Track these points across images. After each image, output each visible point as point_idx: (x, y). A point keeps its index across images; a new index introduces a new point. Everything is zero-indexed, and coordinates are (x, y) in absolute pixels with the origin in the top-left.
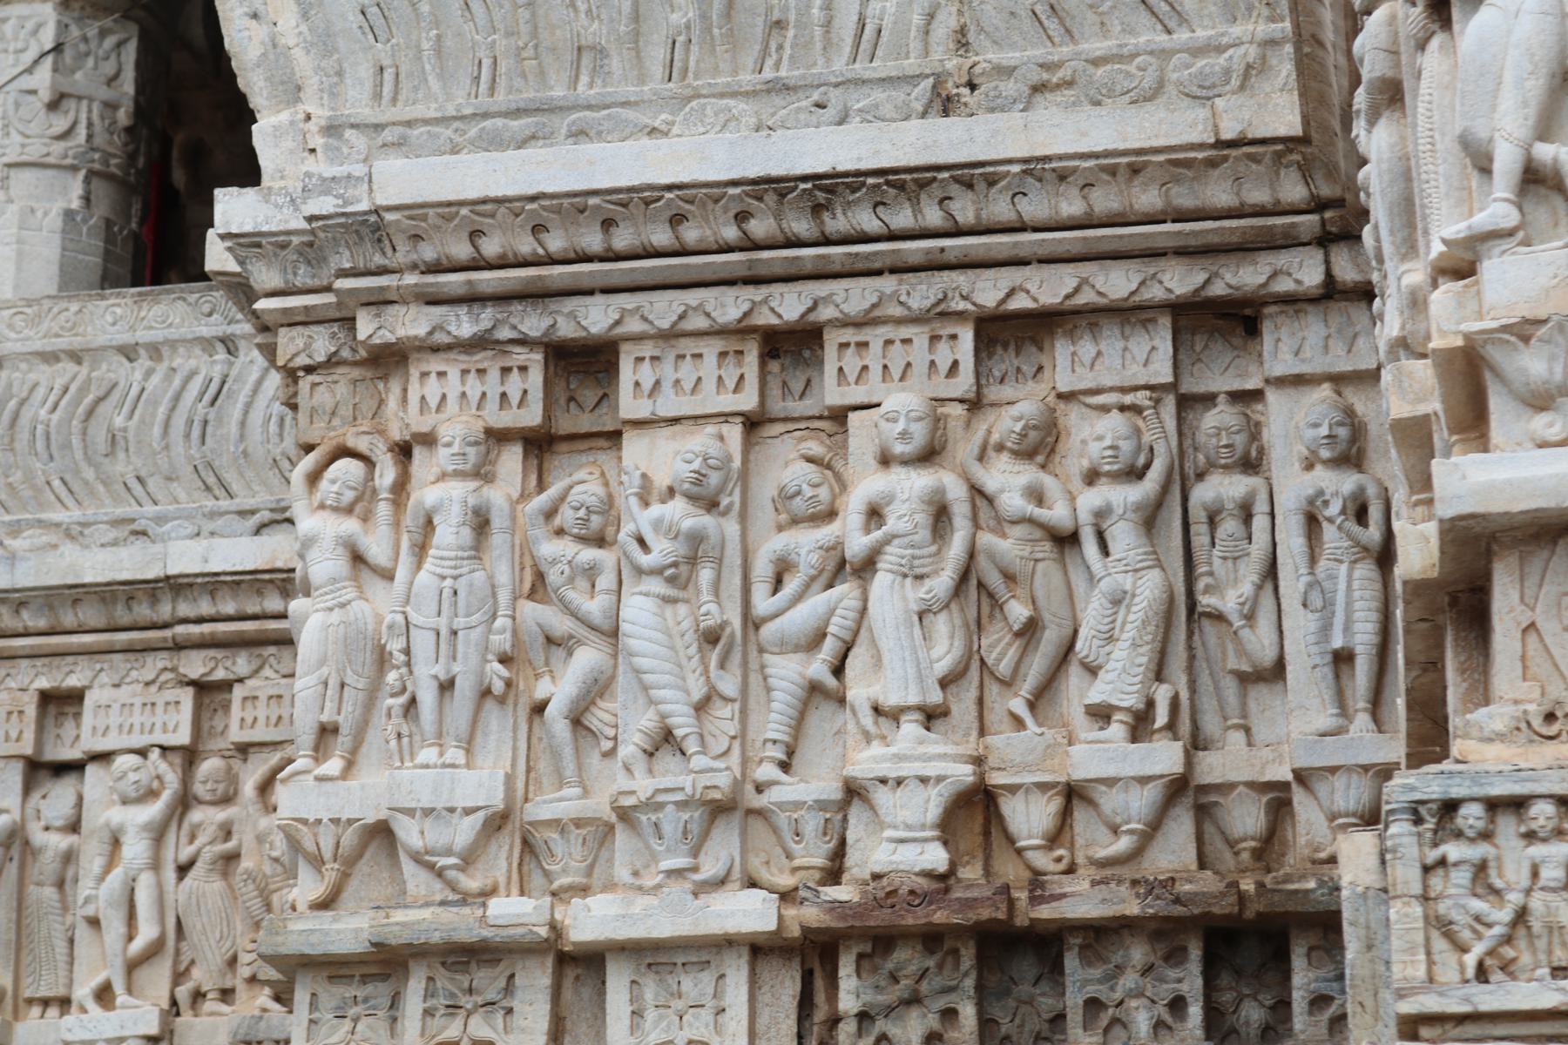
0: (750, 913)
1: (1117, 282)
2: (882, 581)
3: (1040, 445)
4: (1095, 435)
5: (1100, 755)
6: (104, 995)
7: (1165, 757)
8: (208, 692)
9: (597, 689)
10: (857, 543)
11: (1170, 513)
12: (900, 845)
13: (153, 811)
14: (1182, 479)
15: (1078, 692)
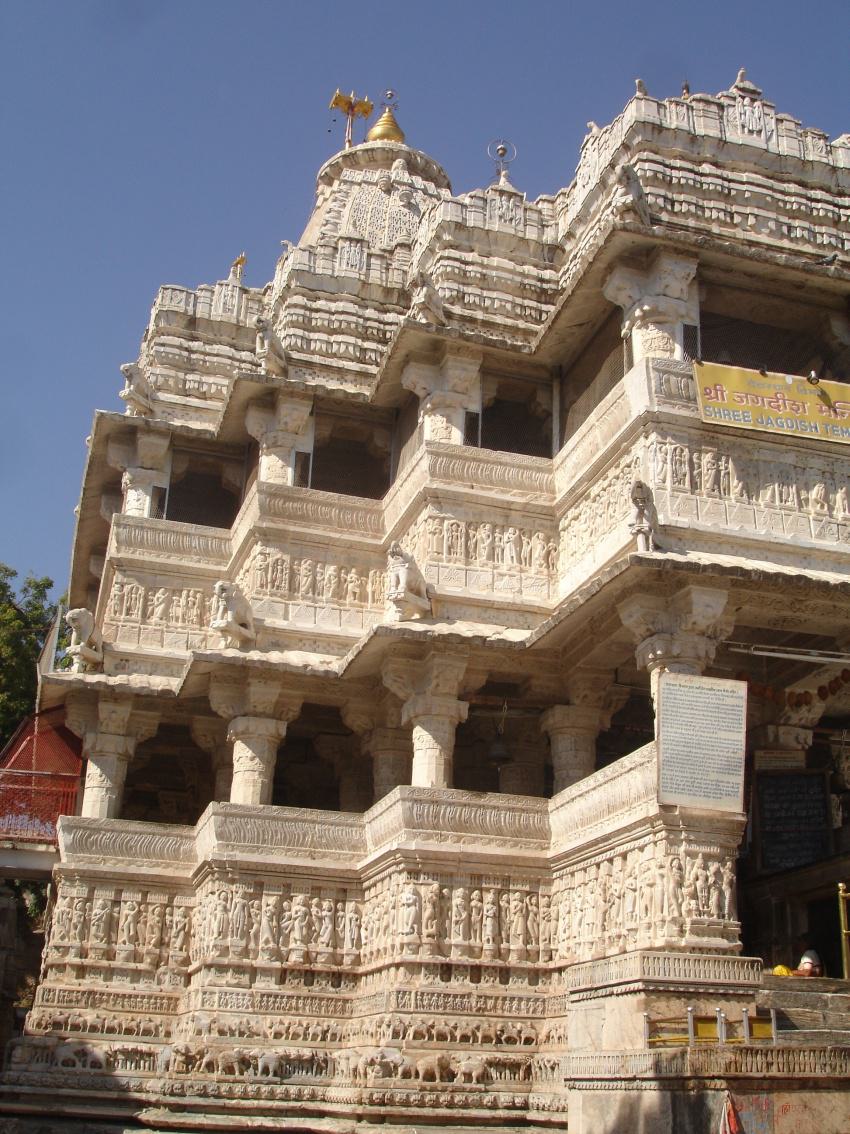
0: (277, 964)
1: (332, 885)
2: (297, 922)
3: (319, 906)
4: (326, 905)
5: (321, 948)
6: (124, 943)
7: (330, 950)
8: (145, 895)
9: (258, 931)
10: (294, 916)
11: (335, 921)
12: (295, 958)
13: (132, 913)
14: (336, 911)
15: (321, 939)
